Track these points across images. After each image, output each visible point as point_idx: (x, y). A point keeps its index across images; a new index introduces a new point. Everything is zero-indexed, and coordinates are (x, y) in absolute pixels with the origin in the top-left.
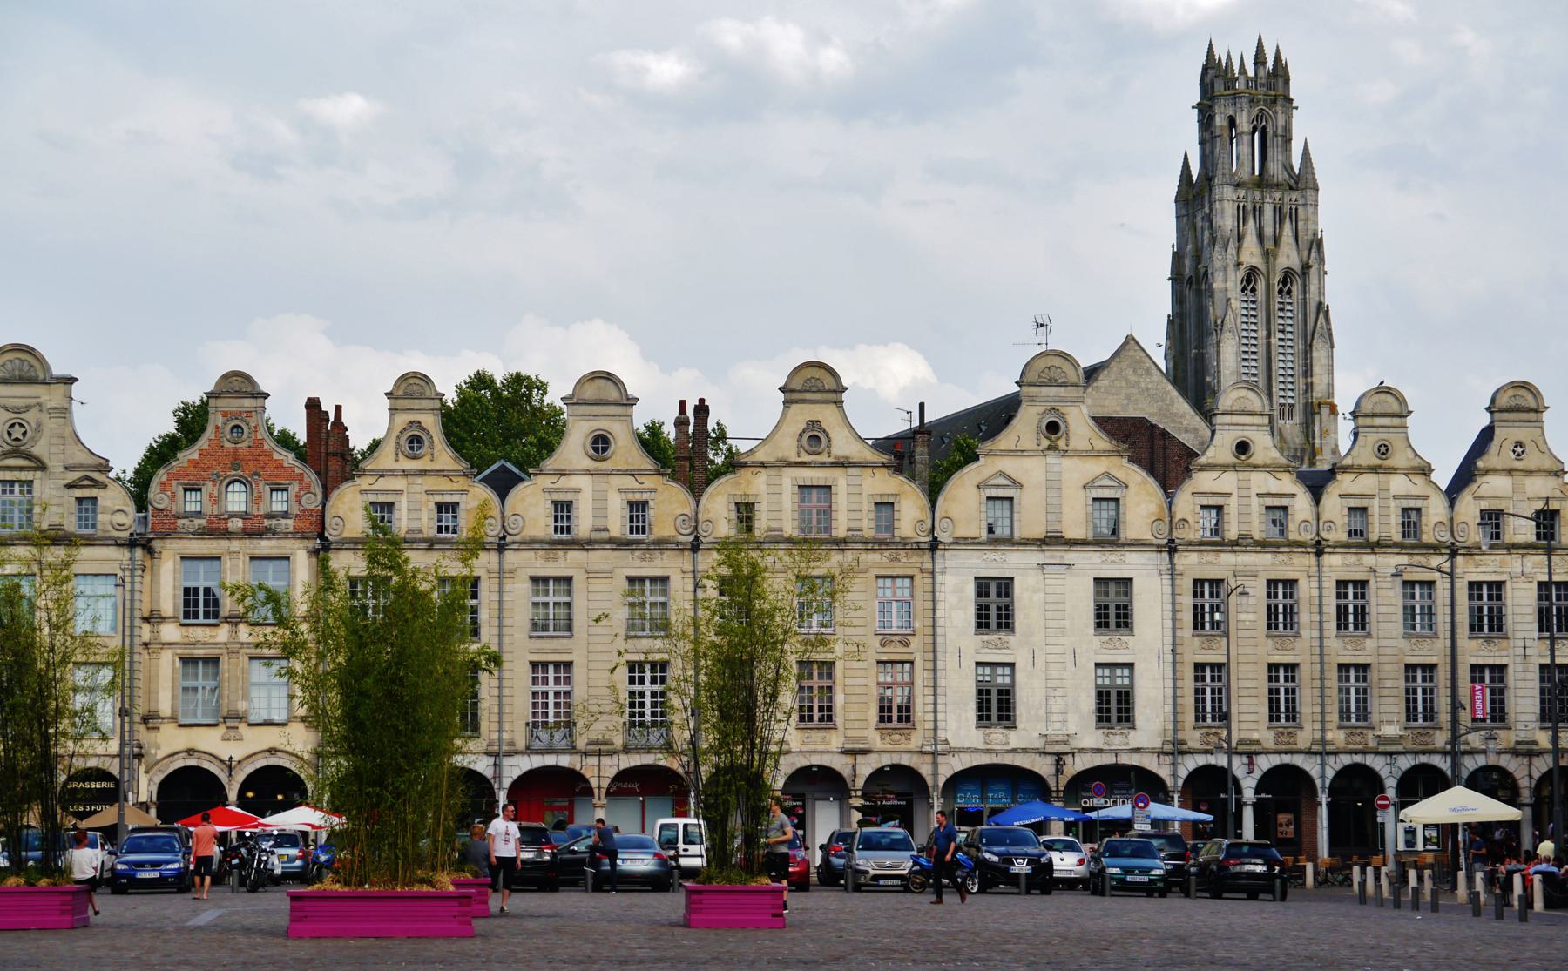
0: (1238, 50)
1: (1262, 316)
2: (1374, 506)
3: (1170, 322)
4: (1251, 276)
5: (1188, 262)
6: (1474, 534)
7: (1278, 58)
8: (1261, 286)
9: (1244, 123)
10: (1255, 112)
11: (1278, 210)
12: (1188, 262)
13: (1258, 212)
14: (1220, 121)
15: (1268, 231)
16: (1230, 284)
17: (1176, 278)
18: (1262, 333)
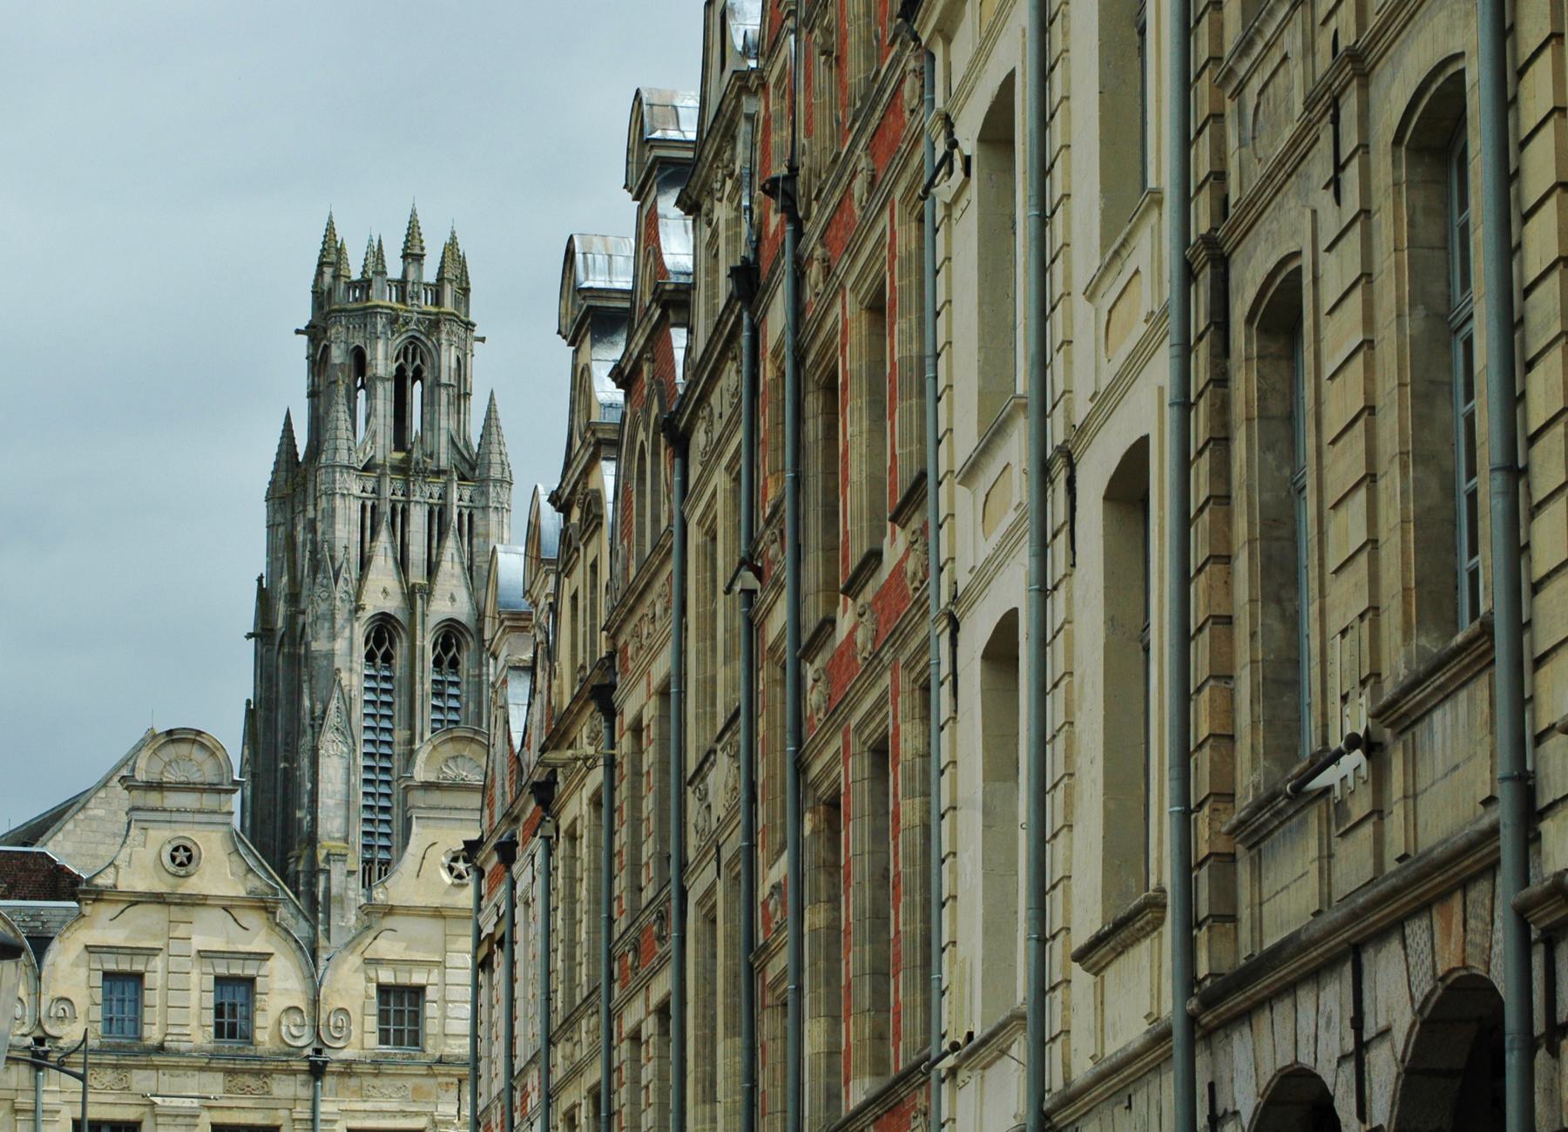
0: (369, 231)
1: (400, 702)
2: (156, 973)
3: (251, 714)
4: (383, 632)
5: (281, 609)
6: (361, 1037)
7: (452, 246)
8: (400, 651)
9: (382, 361)
10: (398, 341)
11: (438, 518)
12: (281, 609)
13: (400, 516)
14: (337, 355)
15: (417, 550)
16: (340, 645)
17: (263, 633)
18: (400, 735)
